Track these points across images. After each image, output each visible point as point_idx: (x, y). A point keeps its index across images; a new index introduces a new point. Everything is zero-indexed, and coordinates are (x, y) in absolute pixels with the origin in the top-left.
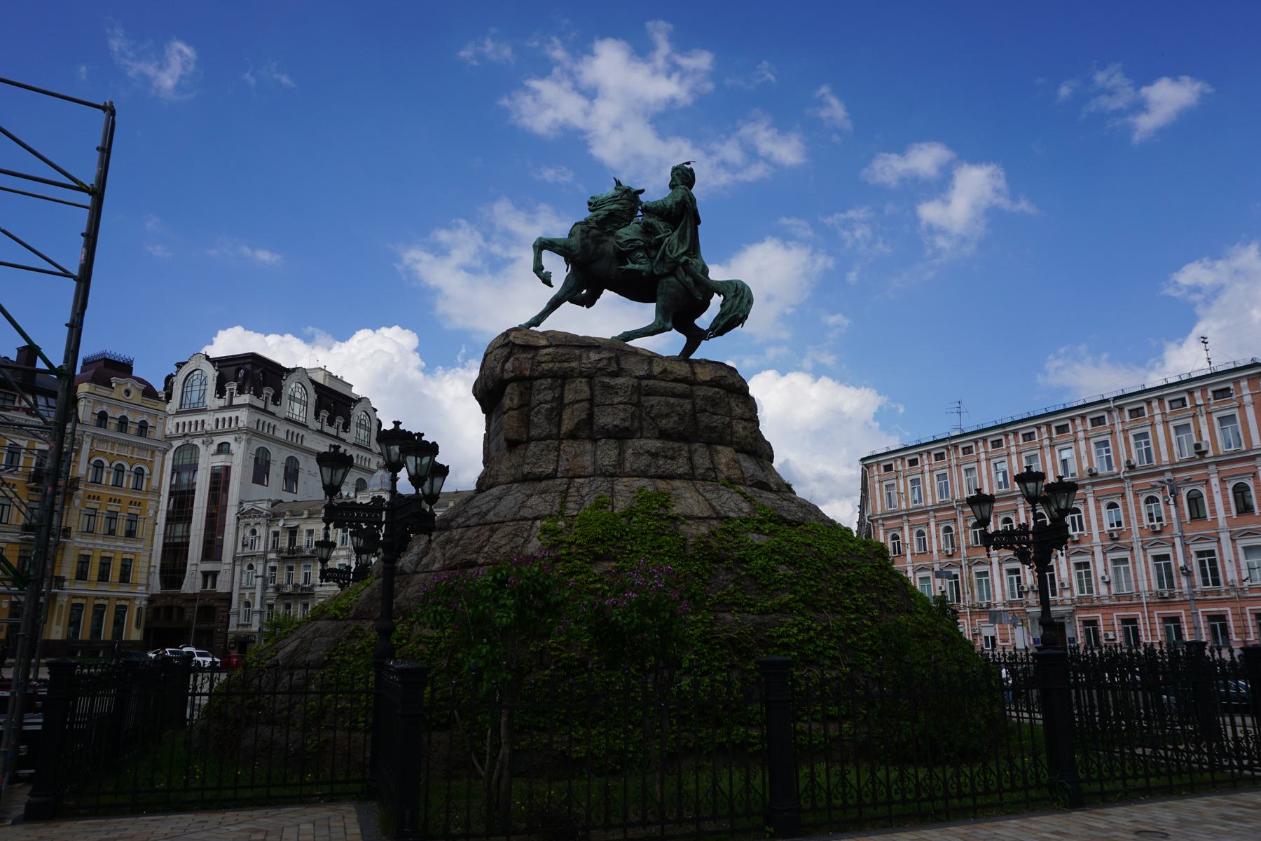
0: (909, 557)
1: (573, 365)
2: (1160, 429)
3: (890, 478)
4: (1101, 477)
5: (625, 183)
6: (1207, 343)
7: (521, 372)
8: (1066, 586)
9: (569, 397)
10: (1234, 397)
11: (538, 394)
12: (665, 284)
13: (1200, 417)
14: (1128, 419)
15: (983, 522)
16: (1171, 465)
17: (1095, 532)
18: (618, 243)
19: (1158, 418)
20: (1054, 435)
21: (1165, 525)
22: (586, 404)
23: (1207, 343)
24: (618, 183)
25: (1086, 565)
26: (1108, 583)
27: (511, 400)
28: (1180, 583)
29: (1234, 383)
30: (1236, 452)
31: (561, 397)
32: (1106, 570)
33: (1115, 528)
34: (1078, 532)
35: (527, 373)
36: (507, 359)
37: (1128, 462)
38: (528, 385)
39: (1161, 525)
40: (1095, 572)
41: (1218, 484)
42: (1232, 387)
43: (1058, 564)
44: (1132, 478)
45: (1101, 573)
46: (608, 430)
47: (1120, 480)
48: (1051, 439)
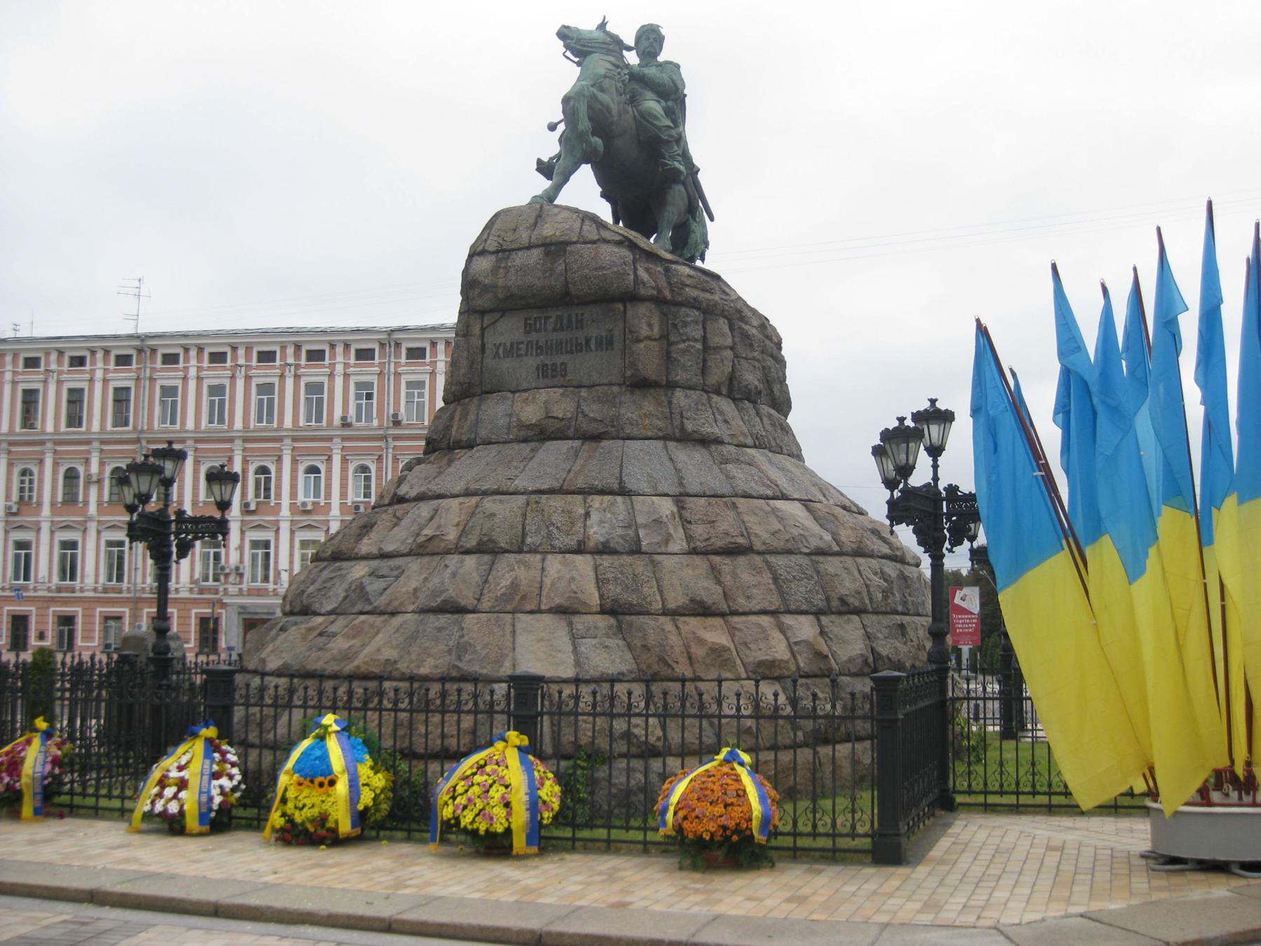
0: (46, 510)
1: (716, 297)
3: (32, 380)
4: (359, 430)
5: (608, 28)
7: (659, 291)
9: (715, 341)
12: (677, 194)
17: (286, 501)
22: (729, 354)
27: (650, 326)
31: (704, 339)
33: (362, 499)
34: (312, 499)
37: (395, 416)
38: (665, 310)
43: (277, 539)
44: (396, 438)
46: (750, 390)
48: (297, 366)
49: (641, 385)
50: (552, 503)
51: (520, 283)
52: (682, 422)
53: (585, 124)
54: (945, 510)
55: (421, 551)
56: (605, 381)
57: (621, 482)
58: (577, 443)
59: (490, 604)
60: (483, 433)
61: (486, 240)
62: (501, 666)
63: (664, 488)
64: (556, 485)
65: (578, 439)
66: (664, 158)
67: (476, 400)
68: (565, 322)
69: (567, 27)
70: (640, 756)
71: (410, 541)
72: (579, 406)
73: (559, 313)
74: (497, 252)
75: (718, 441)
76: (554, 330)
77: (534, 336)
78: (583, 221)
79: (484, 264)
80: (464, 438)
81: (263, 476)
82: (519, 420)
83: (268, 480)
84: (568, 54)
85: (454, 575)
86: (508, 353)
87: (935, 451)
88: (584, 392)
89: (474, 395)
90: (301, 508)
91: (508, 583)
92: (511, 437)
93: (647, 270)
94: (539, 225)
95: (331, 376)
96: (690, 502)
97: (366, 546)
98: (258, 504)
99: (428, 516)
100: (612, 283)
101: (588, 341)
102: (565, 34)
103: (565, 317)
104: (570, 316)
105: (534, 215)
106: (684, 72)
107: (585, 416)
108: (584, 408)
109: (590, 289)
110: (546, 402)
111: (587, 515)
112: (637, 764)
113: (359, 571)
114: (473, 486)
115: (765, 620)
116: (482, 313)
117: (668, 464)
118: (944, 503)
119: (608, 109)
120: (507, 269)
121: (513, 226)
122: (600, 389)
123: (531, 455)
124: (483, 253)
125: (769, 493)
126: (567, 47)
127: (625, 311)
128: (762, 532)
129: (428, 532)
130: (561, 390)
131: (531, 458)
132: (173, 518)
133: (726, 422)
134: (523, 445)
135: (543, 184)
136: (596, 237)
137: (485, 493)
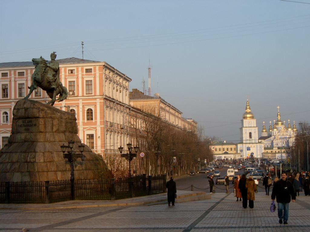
9: (54, 123)
10: (93, 73)
15: (121, 152)
23: (83, 44)
24: (41, 57)
27: (42, 122)
35: (45, 117)
36: (39, 112)
41: (82, 108)
57: (35, 150)
66: (51, 85)
67: (15, 134)
74: (18, 109)
76: (27, 122)
77: (24, 124)
78: (31, 103)
81: (5, 115)
83: (7, 117)
86: (20, 126)
88: (32, 134)
101: (32, 125)
103: (29, 120)
105: (24, 102)
107: (32, 138)
111: (28, 156)
115: (53, 173)
116: (16, 119)
117: (44, 146)
119: (39, 79)
130: (28, 133)
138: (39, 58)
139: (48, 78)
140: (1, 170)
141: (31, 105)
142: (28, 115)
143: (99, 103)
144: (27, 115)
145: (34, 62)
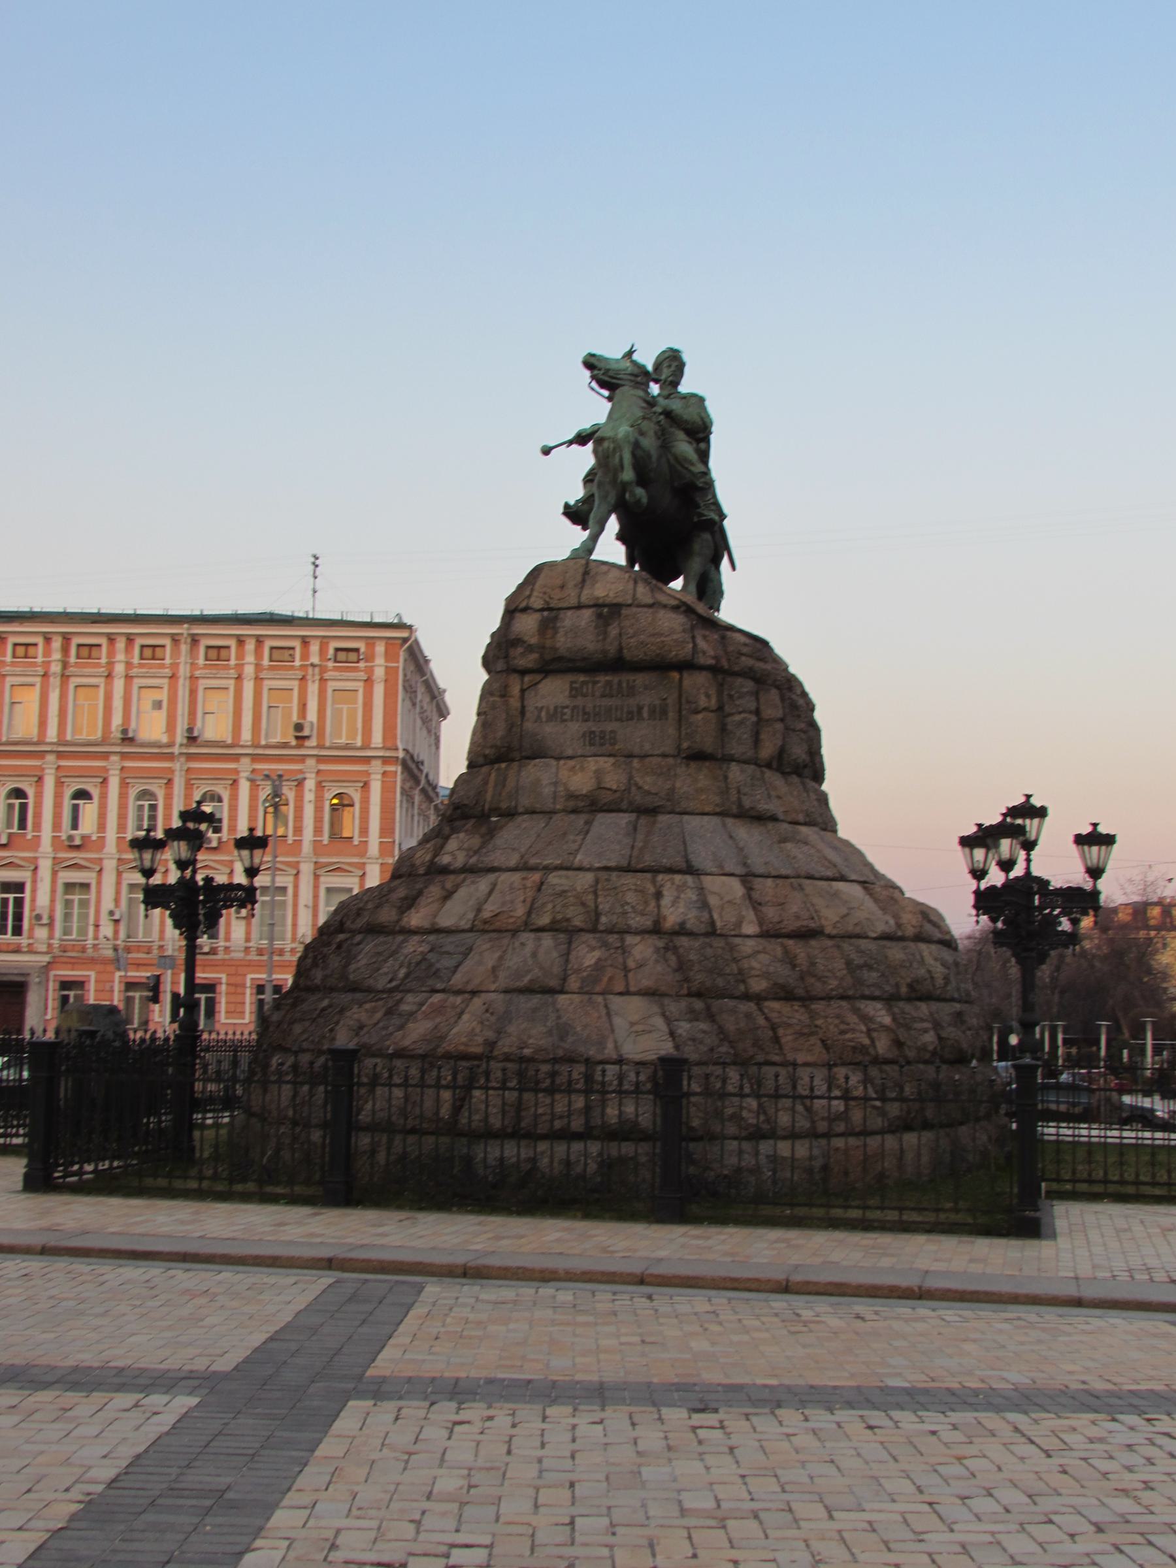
1: (768, 667)
2: (248, 687)
5: (635, 357)
6: (317, 566)
8: (45, 921)
9: (769, 712)
10: (362, 665)
11: (739, 698)
13: (310, 683)
14: (201, 661)
16: (256, 745)
18: (686, 469)
19: (249, 670)
20: (73, 659)
21: (224, 839)
23: (317, 566)
25: (85, 886)
26: (117, 921)
27: (708, 696)
28: (228, 933)
29: (367, 645)
30: (347, 747)
32: (117, 901)
37: (190, 730)
39: (220, 839)
40: (98, 902)
41: (313, 788)
42: (362, 650)
43: (34, 882)
44: (190, 757)
45: (107, 904)
47: (170, 757)
48: (65, 665)
49: (698, 757)
50: (623, 881)
51: (569, 645)
52: (739, 799)
53: (628, 475)
54: (1037, 902)
55: (487, 927)
56: (657, 752)
57: (687, 861)
58: (634, 815)
59: (578, 985)
60: (525, 801)
61: (529, 597)
62: (604, 1048)
63: (730, 867)
64: (624, 863)
65: (632, 812)
67: (516, 763)
68: (615, 687)
69: (593, 355)
70: (749, 1138)
71: (471, 916)
72: (631, 778)
73: (608, 678)
75: (774, 818)
77: (580, 701)
78: (636, 582)
79: (527, 625)
80: (504, 805)
81: (17, 802)
82: (567, 789)
83: (24, 808)
84: (594, 384)
85: (534, 955)
87: (1029, 846)
88: (636, 763)
89: (513, 760)
90: (67, 843)
91: (593, 961)
92: (558, 807)
93: (705, 637)
94: (588, 582)
95: (109, 676)
96: (758, 883)
97: (416, 919)
98: (10, 835)
99: (487, 890)
100: (670, 651)
101: (640, 709)
102: (591, 363)
104: (620, 683)
105: (581, 570)
106: (712, 407)
107: (640, 788)
108: (637, 779)
109: (645, 654)
110: (596, 772)
112: (746, 1145)
113: (414, 947)
114: (533, 861)
116: (523, 672)
118: (1037, 897)
119: (649, 456)
120: (556, 631)
121: (559, 582)
122: (655, 760)
123: (586, 828)
124: (525, 610)
125: (829, 873)
126: (593, 377)
127: (681, 680)
128: (829, 917)
129: (489, 910)
130: (612, 760)
131: (587, 832)
132: (201, 883)
133: (779, 797)
134: (573, 816)
135: (577, 536)
136: (650, 601)
137: (548, 869)
138: (619, 356)
139: (681, 461)
140: (502, 975)
141: (635, 590)
142: (621, 649)
143: (379, 777)
144: (612, 649)
145: (596, 372)
